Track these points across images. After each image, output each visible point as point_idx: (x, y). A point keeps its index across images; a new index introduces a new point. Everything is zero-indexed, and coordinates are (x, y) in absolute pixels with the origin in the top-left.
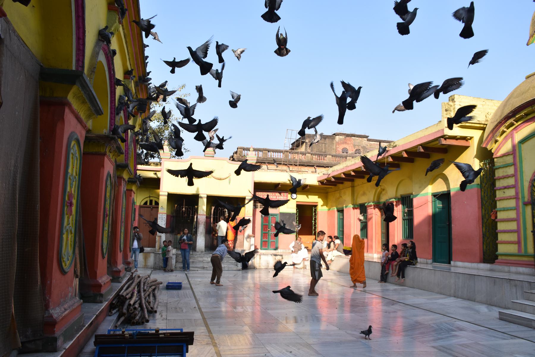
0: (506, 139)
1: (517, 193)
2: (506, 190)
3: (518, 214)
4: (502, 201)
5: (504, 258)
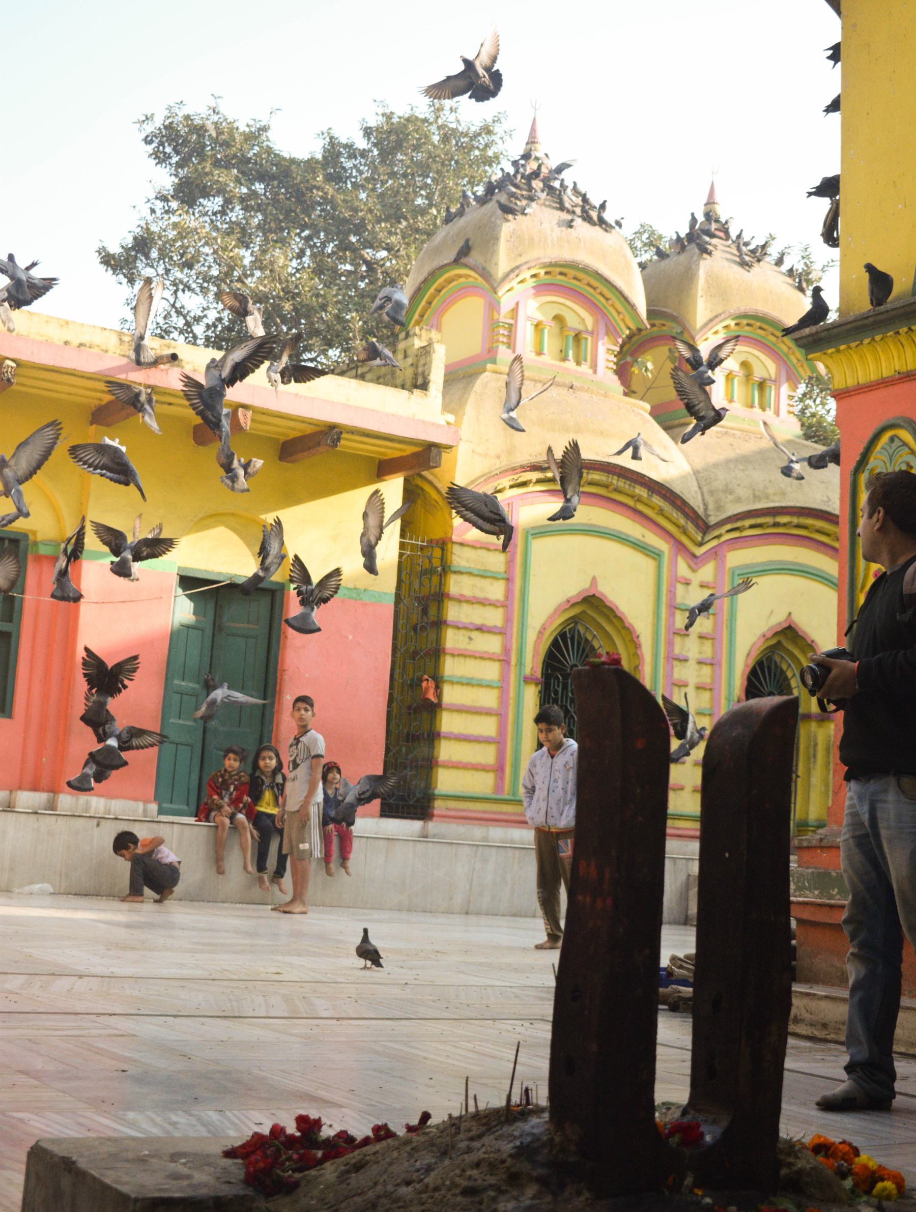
1: (506, 650)
2: (475, 634)
4: (462, 659)
5: (452, 804)
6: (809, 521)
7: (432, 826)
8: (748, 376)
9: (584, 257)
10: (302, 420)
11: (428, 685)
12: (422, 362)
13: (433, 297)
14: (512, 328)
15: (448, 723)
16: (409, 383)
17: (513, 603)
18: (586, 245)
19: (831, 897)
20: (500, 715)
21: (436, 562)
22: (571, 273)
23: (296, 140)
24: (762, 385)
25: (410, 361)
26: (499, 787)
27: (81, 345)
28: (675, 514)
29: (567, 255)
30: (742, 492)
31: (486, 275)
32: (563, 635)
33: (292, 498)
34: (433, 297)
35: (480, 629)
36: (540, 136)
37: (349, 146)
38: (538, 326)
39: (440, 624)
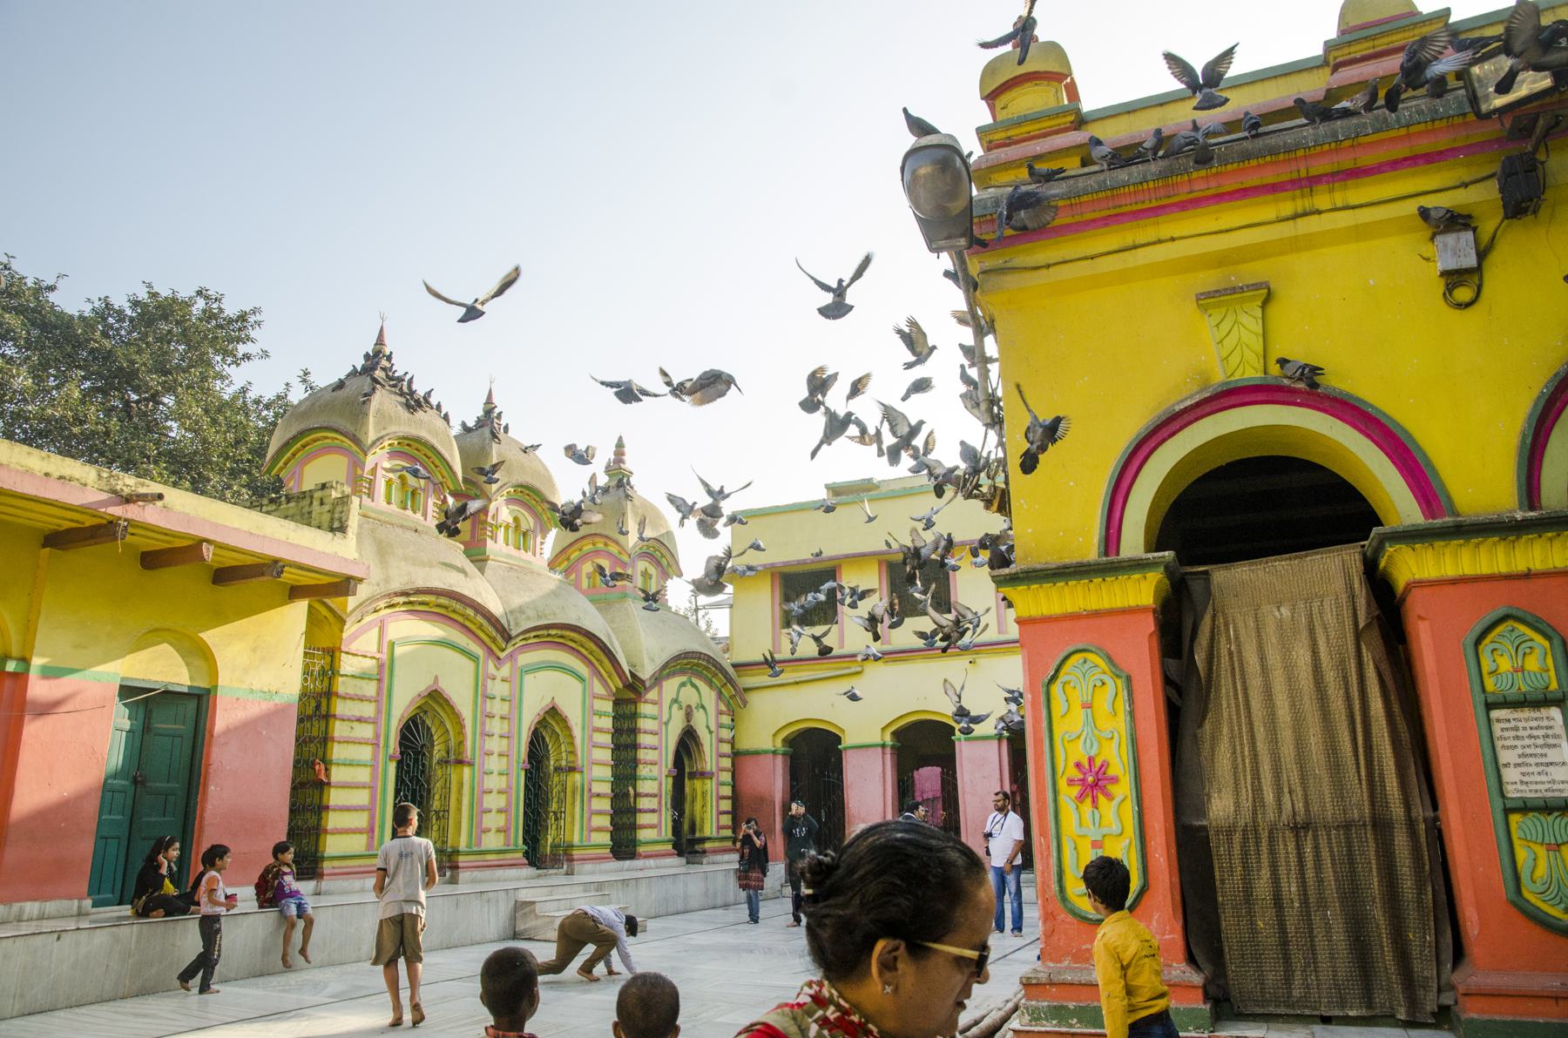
0: (370, 626)
1: (377, 736)
2: (355, 724)
3: (374, 775)
5: (336, 863)
6: (568, 633)
7: (325, 884)
8: (517, 527)
9: (424, 434)
10: (252, 554)
11: (320, 767)
12: (339, 509)
13: (299, 450)
14: (371, 483)
15: (335, 797)
16: (326, 525)
17: (383, 698)
18: (422, 425)
19: (1071, 1026)
20: (372, 788)
21: (327, 667)
22: (416, 445)
23: (72, 301)
24: (525, 534)
25: (327, 508)
26: (370, 846)
27: (61, 478)
28: (491, 629)
29: (414, 431)
30: (530, 613)
31: (356, 440)
32: (413, 719)
33: (220, 617)
34: (299, 450)
35: (359, 720)
36: (387, 340)
37: (120, 312)
38: (389, 483)
39: (328, 717)
